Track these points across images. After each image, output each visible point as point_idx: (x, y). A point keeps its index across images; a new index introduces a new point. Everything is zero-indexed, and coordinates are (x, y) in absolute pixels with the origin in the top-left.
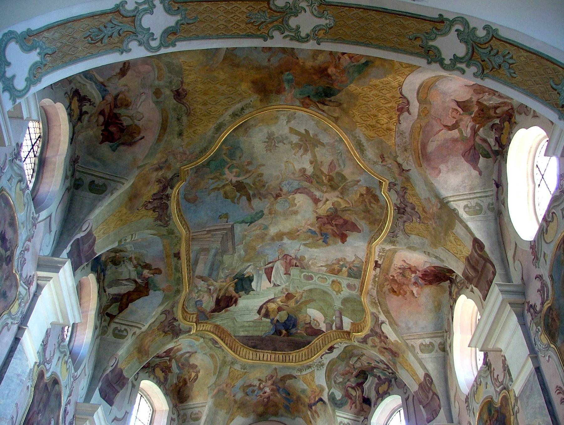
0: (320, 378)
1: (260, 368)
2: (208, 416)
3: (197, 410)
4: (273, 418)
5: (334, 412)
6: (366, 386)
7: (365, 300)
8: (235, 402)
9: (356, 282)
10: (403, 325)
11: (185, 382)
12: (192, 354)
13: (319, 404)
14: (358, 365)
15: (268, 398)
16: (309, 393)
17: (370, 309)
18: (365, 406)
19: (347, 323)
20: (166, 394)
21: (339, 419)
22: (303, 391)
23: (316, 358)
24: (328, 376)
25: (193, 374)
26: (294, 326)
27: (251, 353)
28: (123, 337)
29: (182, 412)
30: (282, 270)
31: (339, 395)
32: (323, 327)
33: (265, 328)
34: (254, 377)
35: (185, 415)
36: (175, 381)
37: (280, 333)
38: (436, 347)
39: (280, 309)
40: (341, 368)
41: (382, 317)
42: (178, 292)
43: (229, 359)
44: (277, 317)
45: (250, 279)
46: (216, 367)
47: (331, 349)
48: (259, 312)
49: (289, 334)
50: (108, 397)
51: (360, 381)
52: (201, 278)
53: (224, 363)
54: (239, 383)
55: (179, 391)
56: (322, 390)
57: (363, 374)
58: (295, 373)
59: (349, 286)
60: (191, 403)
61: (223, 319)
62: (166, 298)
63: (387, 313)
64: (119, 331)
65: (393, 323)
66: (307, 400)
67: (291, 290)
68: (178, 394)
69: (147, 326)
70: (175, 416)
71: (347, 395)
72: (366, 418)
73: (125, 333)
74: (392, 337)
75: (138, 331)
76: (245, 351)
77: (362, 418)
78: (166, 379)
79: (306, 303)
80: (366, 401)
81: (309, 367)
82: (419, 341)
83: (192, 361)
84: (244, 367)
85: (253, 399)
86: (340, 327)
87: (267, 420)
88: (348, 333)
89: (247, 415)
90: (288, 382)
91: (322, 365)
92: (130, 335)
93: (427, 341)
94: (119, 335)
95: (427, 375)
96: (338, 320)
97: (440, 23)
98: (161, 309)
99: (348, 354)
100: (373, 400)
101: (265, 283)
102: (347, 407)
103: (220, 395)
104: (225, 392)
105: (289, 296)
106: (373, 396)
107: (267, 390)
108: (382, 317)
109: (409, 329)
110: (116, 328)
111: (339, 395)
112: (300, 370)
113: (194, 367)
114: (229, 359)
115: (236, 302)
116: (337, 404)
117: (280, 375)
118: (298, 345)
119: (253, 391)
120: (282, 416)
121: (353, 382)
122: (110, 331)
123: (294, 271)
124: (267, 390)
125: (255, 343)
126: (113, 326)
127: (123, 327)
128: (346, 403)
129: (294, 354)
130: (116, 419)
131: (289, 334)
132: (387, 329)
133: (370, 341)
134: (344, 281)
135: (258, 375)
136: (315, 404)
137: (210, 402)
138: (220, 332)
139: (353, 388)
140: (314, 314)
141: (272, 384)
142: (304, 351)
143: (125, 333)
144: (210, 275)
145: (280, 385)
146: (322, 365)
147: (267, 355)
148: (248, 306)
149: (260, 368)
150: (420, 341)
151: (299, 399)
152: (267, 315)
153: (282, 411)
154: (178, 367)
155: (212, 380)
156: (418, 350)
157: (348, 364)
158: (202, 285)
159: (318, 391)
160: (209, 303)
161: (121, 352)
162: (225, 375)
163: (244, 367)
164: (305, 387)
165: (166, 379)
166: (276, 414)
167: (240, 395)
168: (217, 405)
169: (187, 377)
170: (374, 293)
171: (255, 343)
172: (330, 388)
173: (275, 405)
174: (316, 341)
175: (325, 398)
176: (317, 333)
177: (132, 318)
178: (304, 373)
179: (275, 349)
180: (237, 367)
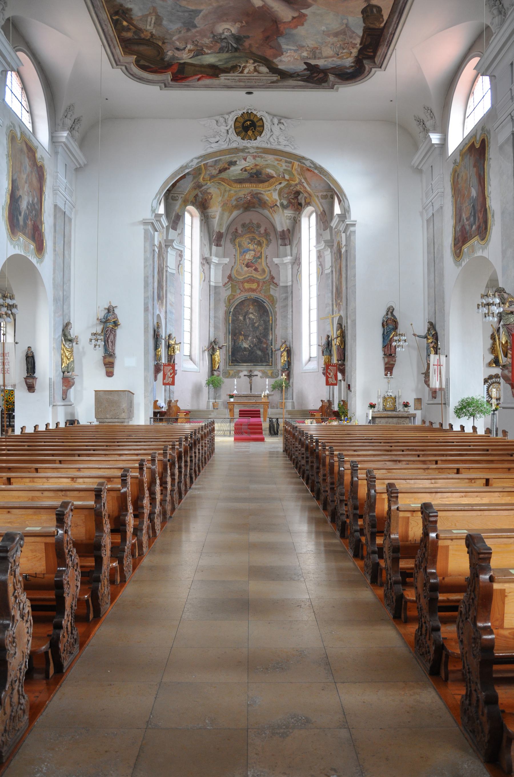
0: (275, 196)
1: (245, 191)
2: (219, 216)
3: (213, 214)
4: (252, 209)
5: (283, 211)
6: (299, 197)
7: (295, 173)
8: (233, 206)
9: (290, 165)
10: (313, 185)
11: (206, 200)
12: (208, 189)
13: (276, 207)
14: (295, 189)
15: (250, 200)
16: (270, 201)
17: (297, 176)
18: (299, 207)
19: (287, 177)
20: (197, 208)
21: (286, 215)
22: (267, 200)
23: (273, 187)
24: (280, 194)
25: (210, 197)
26: (260, 174)
27: (239, 186)
28: (177, 200)
29: (206, 214)
30: (252, 158)
31: (285, 203)
32: (275, 176)
33: (245, 175)
34: (241, 194)
35: (208, 216)
36: (200, 200)
37: (253, 177)
38: (329, 196)
39: (252, 169)
40: (286, 190)
41: (303, 180)
42: (200, 174)
43: (227, 189)
44: (251, 171)
45: (236, 162)
46: (221, 193)
47: (280, 183)
48: (241, 170)
49: (257, 177)
50: (175, 228)
51: (296, 195)
52: (211, 166)
53: (225, 191)
54: (234, 198)
55: (203, 205)
56: (277, 201)
57: (298, 193)
58: (262, 192)
59: (286, 166)
60: (210, 210)
61: (224, 175)
62: (194, 178)
63: (305, 179)
64: (175, 197)
65: (308, 184)
66: (269, 205)
67: (257, 163)
68: (203, 206)
69: (187, 192)
70: (203, 218)
71: (290, 202)
72: (299, 213)
73: (177, 198)
74: (308, 189)
75: (183, 196)
76: (235, 185)
77: (298, 213)
78: (196, 200)
79: (265, 168)
80: (300, 204)
81: (269, 191)
82: (321, 194)
83: (209, 191)
84: (235, 192)
85: (242, 202)
86: (284, 177)
87: (250, 211)
88: (288, 180)
89: (239, 209)
90: (259, 195)
91: (276, 190)
92: (180, 198)
93: (325, 193)
94: (174, 199)
95: (324, 211)
96: (283, 175)
97: (303, 158)
98: (193, 183)
99: (288, 186)
100: (303, 204)
101: (243, 162)
102: (290, 208)
103: (224, 206)
104: (227, 204)
105: (256, 165)
106: (303, 202)
107: (249, 198)
108: (303, 180)
109: (316, 187)
110: (173, 196)
111: (285, 203)
112: (265, 192)
113: (210, 193)
114: (227, 189)
115: (229, 169)
116: (284, 207)
117: (255, 192)
118: (263, 182)
119: (241, 200)
120: (257, 208)
121: (292, 196)
122: (170, 198)
123: (257, 159)
124: (249, 198)
125: (240, 181)
126: (171, 195)
127: (176, 195)
128: (289, 206)
129: (261, 185)
130: (179, 234)
131: (257, 177)
132: (305, 184)
133: (298, 186)
134: (284, 165)
135: (243, 193)
136: (273, 207)
137: (219, 209)
138: (223, 180)
139: (293, 199)
140: (270, 171)
141: (251, 195)
142: (266, 184)
143: (177, 198)
144: (215, 165)
145: (255, 196)
146: (276, 190)
147: (247, 185)
148: (235, 171)
149: (245, 191)
150: (322, 193)
151: (265, 203)
152: (246, 170)
153: (257, 206)
154: (201, 194)
155: (220, 199)
156: (320, 198)
157: (289, 189)
158: (211, 168)
159: (274, 201)
160: (214, 172)
161: (177, 207)
162: (226, 196)
163: (235, 192)
164: (268, 199)
165: (196, 200)
166: (254, 207)
167: (234, 203)
168: (223, 210)
169: (206, 198)
170: (299, 170)
171: (240, 181)
172: (280, 200)
173: (254, 203)
174: (272, 180)
175: (278, 204)
176: (273, 177)
177: (179, 190)
178: (267, 193)
179: (251, 183)
180: (232, 192)
